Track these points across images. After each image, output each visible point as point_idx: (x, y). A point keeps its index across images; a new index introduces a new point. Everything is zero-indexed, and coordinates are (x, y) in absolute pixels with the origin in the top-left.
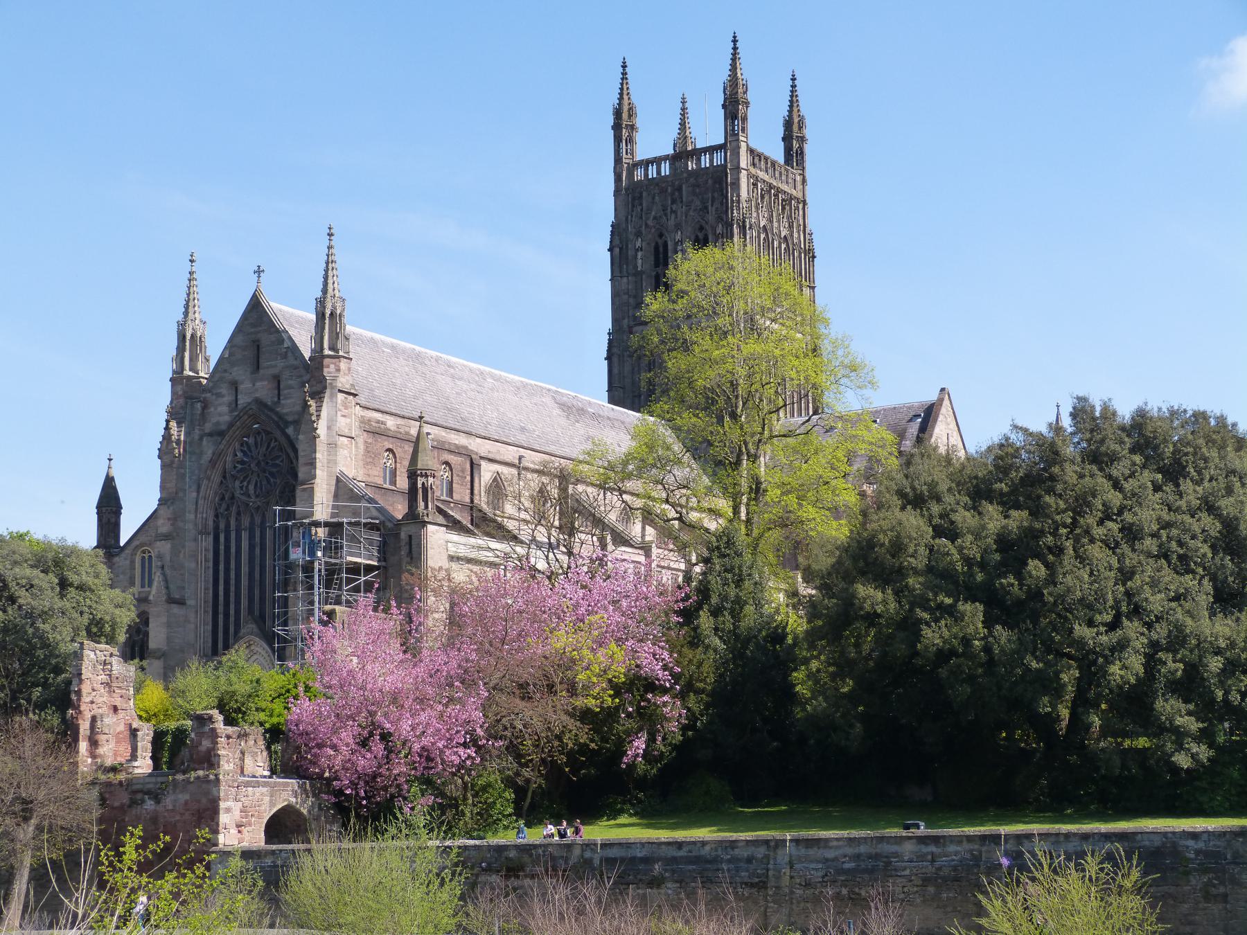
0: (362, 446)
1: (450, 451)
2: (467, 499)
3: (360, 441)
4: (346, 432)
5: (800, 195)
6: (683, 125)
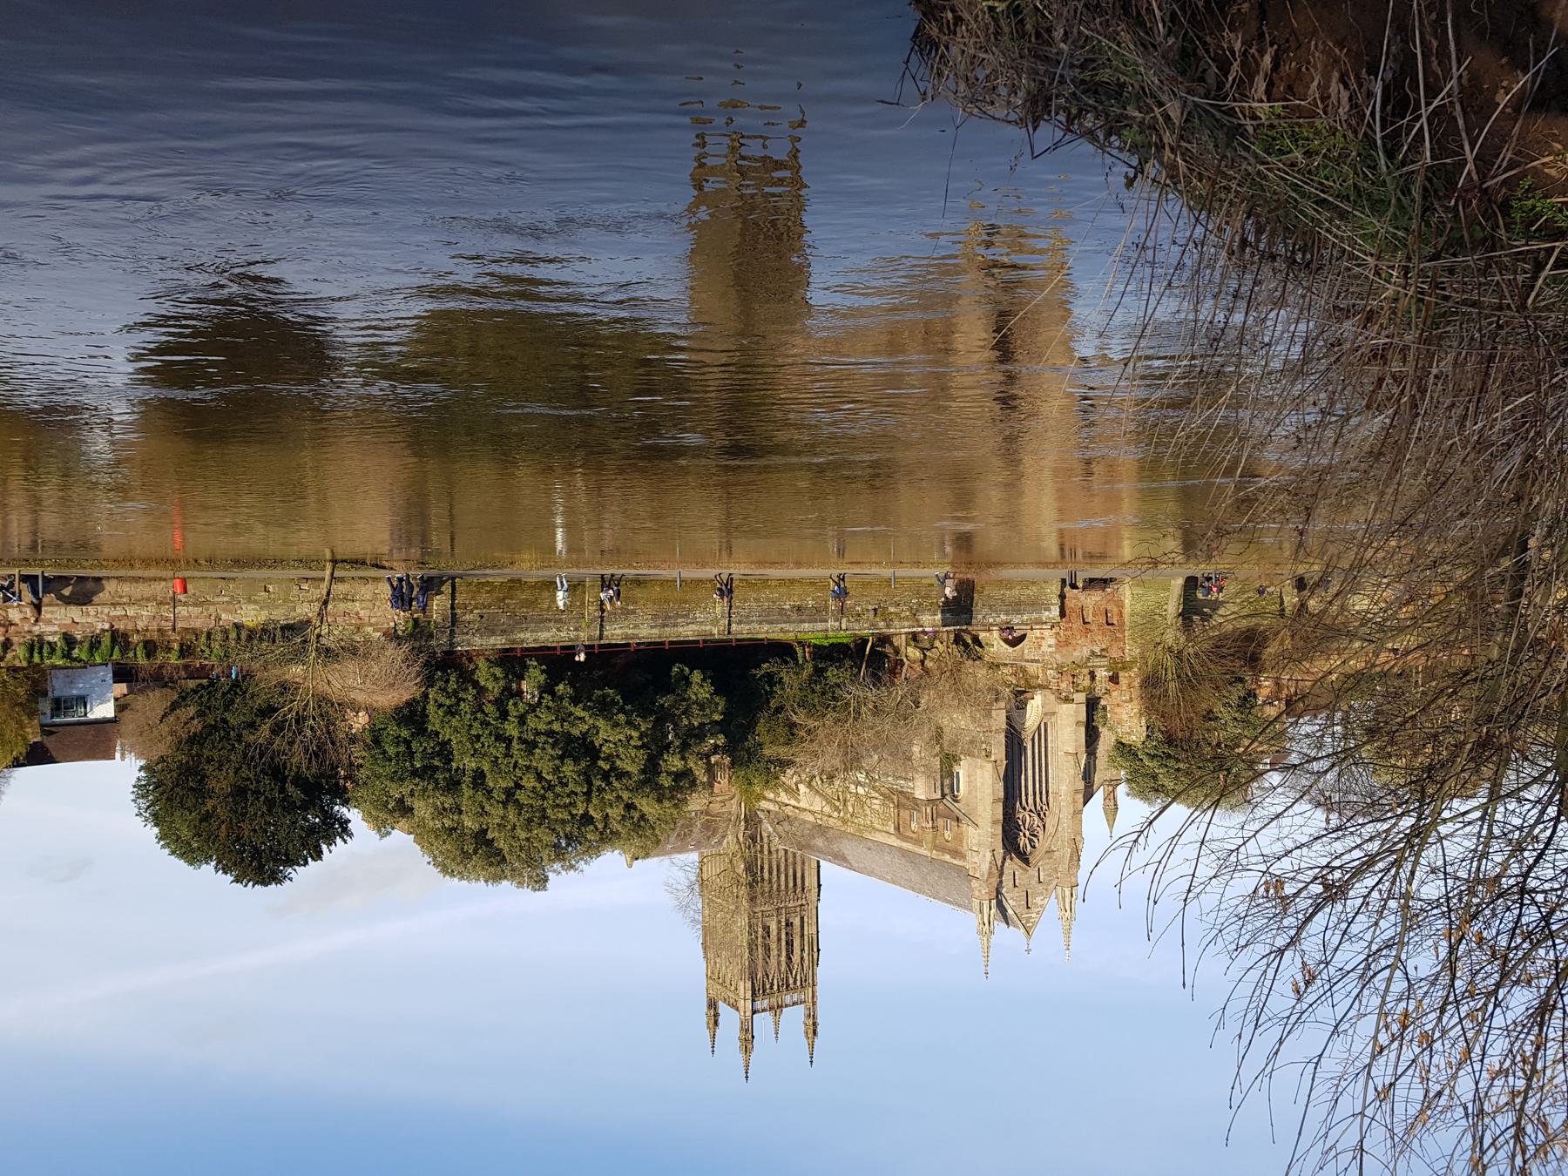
0: (965, 844)
1: (912, 838)
2: (902, 811)
3: (965, 847)
4: (974, 854)
5: (710, 981)
6: (777, 1024)
